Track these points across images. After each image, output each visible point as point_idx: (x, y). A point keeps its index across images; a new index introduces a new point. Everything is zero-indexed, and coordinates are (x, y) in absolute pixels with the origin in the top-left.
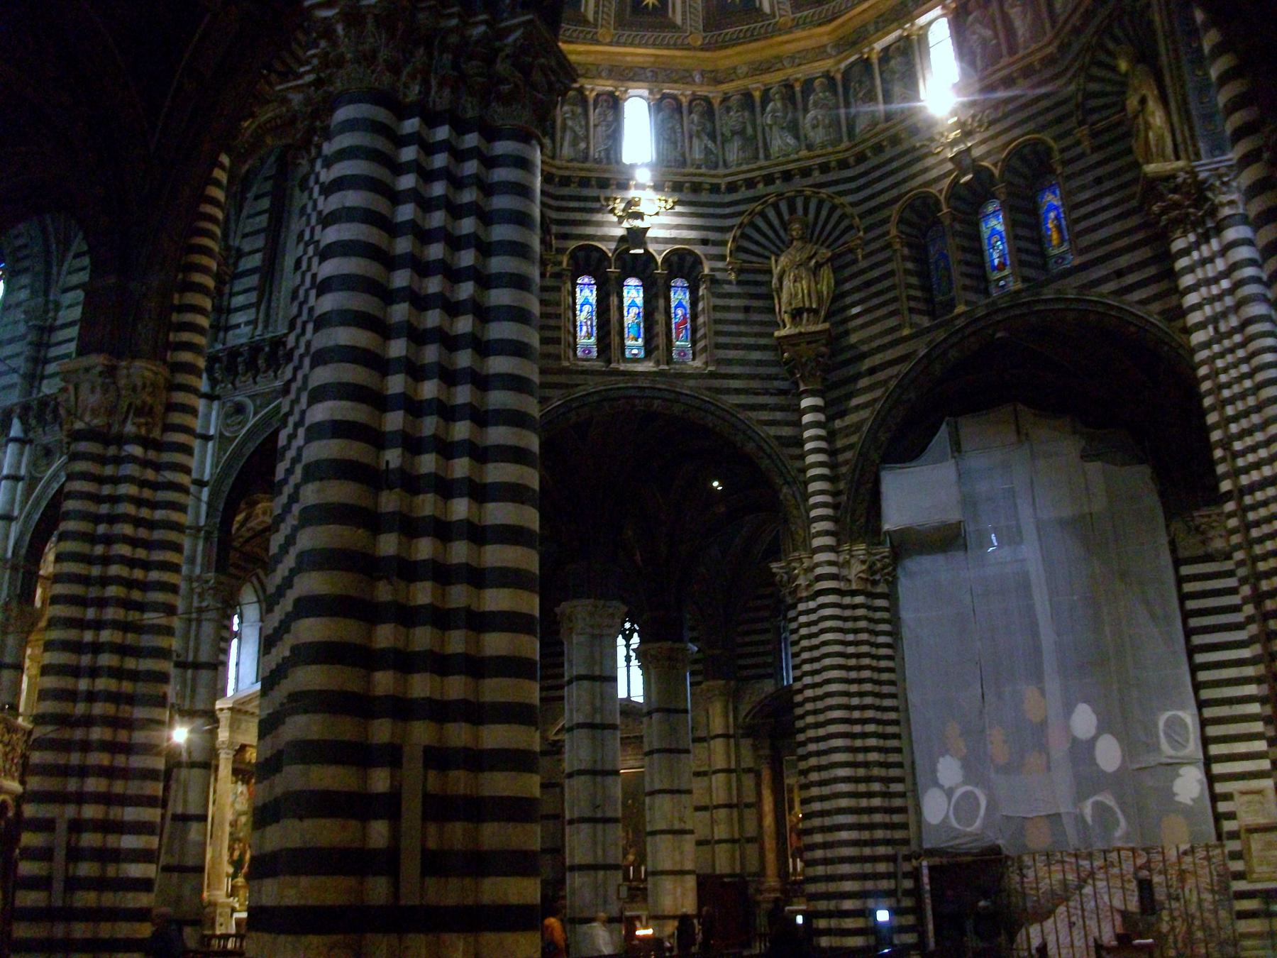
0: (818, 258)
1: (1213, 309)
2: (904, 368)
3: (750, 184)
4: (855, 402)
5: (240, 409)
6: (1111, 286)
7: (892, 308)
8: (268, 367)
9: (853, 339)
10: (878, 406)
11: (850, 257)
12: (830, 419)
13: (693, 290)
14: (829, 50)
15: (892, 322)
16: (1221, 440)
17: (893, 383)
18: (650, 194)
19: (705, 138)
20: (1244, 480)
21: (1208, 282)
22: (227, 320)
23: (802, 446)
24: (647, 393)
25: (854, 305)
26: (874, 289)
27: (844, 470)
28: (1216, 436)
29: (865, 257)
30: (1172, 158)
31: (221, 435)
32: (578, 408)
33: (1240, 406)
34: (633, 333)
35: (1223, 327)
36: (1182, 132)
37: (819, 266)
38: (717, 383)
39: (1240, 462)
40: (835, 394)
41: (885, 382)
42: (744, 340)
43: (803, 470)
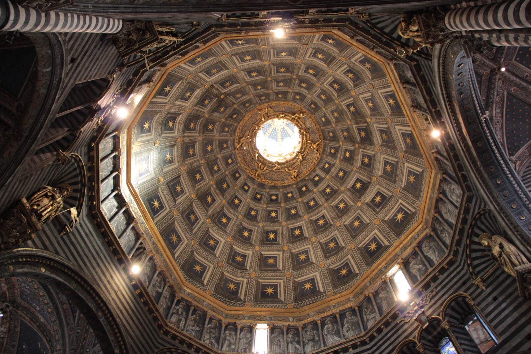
14: (351, 299)
19: (295, 344)
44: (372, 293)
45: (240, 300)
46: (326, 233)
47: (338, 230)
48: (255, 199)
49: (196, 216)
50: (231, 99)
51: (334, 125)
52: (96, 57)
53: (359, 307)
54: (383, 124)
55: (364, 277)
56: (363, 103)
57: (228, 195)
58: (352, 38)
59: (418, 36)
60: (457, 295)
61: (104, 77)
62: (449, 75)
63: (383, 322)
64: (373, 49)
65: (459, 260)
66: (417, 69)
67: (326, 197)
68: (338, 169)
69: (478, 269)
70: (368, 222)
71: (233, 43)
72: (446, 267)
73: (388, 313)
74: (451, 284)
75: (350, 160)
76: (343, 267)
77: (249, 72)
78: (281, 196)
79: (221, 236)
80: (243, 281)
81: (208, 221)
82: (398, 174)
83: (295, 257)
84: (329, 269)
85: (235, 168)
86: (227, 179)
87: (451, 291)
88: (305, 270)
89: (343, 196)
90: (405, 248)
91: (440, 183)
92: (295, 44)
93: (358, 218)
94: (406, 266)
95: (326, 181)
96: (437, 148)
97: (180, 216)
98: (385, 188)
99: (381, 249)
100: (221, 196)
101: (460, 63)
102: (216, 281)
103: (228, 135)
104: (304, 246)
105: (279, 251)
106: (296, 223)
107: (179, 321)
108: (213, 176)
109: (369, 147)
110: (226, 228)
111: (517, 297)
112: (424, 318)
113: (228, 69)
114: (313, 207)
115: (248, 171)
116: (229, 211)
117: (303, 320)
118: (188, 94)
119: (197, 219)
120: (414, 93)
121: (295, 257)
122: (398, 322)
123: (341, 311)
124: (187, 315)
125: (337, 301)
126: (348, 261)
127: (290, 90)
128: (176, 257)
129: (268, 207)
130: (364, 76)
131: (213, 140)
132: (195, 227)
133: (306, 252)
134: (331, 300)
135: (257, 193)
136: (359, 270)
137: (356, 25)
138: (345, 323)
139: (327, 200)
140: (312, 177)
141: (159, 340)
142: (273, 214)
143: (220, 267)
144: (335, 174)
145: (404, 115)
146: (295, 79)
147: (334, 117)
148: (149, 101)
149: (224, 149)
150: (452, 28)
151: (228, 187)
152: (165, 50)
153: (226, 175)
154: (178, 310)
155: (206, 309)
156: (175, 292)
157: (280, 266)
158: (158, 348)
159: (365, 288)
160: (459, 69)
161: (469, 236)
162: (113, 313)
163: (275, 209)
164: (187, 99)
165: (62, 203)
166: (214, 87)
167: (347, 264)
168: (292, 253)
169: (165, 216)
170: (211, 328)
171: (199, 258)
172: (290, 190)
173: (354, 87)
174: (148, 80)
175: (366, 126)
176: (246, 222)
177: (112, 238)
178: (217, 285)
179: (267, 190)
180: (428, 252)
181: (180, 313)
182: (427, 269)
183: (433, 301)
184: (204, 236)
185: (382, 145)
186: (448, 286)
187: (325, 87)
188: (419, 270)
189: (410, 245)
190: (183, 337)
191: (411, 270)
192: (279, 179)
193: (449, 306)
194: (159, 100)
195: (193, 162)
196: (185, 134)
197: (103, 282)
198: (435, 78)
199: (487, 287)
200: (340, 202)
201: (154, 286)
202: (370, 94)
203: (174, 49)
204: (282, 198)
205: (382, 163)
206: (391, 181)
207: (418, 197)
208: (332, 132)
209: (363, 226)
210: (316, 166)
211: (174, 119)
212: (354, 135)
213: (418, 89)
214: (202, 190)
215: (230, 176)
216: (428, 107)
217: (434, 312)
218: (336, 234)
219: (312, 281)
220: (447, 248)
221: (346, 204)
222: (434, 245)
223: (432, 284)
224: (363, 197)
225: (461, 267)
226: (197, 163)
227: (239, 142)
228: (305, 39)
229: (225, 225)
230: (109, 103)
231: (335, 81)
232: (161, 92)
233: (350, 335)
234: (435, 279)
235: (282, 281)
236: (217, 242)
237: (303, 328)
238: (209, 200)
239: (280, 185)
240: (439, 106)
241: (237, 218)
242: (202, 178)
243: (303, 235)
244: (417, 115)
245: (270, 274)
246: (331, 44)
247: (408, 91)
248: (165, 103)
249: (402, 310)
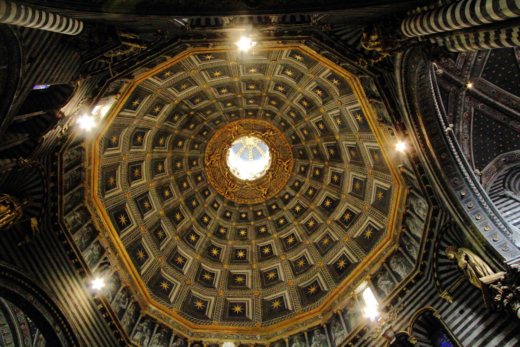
14: (319, 317)
44: (340, 310)
45: (207, 318)
47: (307, 248)
48: (224, 217)
49: (164, 233)
50: (201, 115)
51: (304, 143)
52: (57, 60)
54: (351, 141)
55: (333, 294)
56: (332, 120)
57: (198, 212)
58: (318, 52)
59: (378, 46)
60: (424, 310)
61: (67, 83)
62: (412, 86)
63: (351, 339)
64: (339, 64)
65: (426, 276)
66: (381, 83)
67: (295, 215)
69: (444, 283)
70: (338, 239)
71: (201, 57)
72: (413, 281)
73: (356, 330)
74: (418, 298)
75: (319, 178)
76: (312, 285)
77: (219, 88)
78: (250, 214)
79: (189, 254)
81: (177, 238)
83: (263, 276)
84: (298, 287)
85: (205, 185)
86: (197, 197)
87: (418, 306)
88: (274, 288)
89: (313, 214)
90: (373, 265)
91: (407, 198)
92: (264, 60)
93: (327, 236)
94: (374, 281)
95: (296, 199)
96: (404, 163)
97: (147, 232)
98: (355, 206)
99: (349, 266)
100: (190, 214)
101: (422, 73)
103: (197, 152)
104: (273, 264)
105: (248, 269)
106: (265, 241)
107: (143, 338)
108: (182, 193)
109: (338, 165)
110: (194, 246)
111: (484, 309)
113: (198, 85)
114: (282, 225)
115: (217, 189)
116: (198, 229)
117: (270, 338)
118: (157, 109)
120: (380, 108)
121: (263, 276)
122: (366, 339)
123: (309, 329)
124: (152, 333)
125: (305, 319)
127: (261, 108)
128: (142, 274)
129: (237, 225)
130: (332, 92)
131: (182, 157)
132: (163, 243)
133: (275, 270)
134: (300, 318)
135: (227, 211)
136: (328, 288)
137: (320, 38)
138: (313, 341)
139: (296, 218)
140: (282, 195)
142: (243, 233)
143: (188, 285)
144: (304, 192)
145: (371, 131)
146: (265, 96)
147: (304, 134)
148: (116, 114)
149: (194, 166)
150: (410, 35)
151: (198, 204)
152: (131, 60)
153: (196, 193)
154: (142, 328)
155: (171, 327)
156: (140, 309)
157: (249, 284)
160: (421, 80)
161: (436, 250)
162: (72, 327)
163: (244, 227)
164: (156, 114)
165: (21, 211)
166: (183, 103)
167: (316, 281)
168: (261, 272)
169: (132, 231)
172: (260, 209)
173: (323, 104)
174: (115, 92)
175: (335, 144)
177: (75, 251)
179: (237, 209)
180: (396, 268)
181: (144, 330)
182: (394, 284)
183: (400, 316)
185: (351, 162)
186: (416, 301)
187: (295, 105)
188: (387, 286)
191: (379, 286)
192: (249, 197)
193: (416, 321)
194: (127, 113)
195: (162, 178)
196: (154, 150)
197: (62, 296)
198: (397, 89)
199: (454, 301)
200: (310, 220)
201: (118, 302)
202: (338, 111)
203: (140, 59)
204: (252, 216)
205: (351, 180)
206: (360, 198)
207: (386, 213)
208: (302, 150)
209: (333, 244)
210: (286, 184)
211: (143, 135)
212: (323, 152)
213: (383, 103)
214: (171, 207)
216: (392, 119)
217: (401, 327)
218: (305, 252)
219: (281, 299)
220: (414, 263)
221: (315, 221)
222: (402, 261)
223: (400, 299)
225: (428, 282)
226: (167, 180)
227: (209, 159)
228: (273, 55)
229: (194, 243)
230: (73, 112)
231: (305, 98)
232: (129, 106)
234: (402, 294)
235: (250, 300)
236: (185, 260)
238: (178, 217)
239: (249, 203)
240: (403, 118)
241: (206, 236)
242: (171, 195)
243: (273, 253)
244: (382, 129)
245: (238, 292)
246: (299, 60)
247: (375, 105)
248: (134, 117)
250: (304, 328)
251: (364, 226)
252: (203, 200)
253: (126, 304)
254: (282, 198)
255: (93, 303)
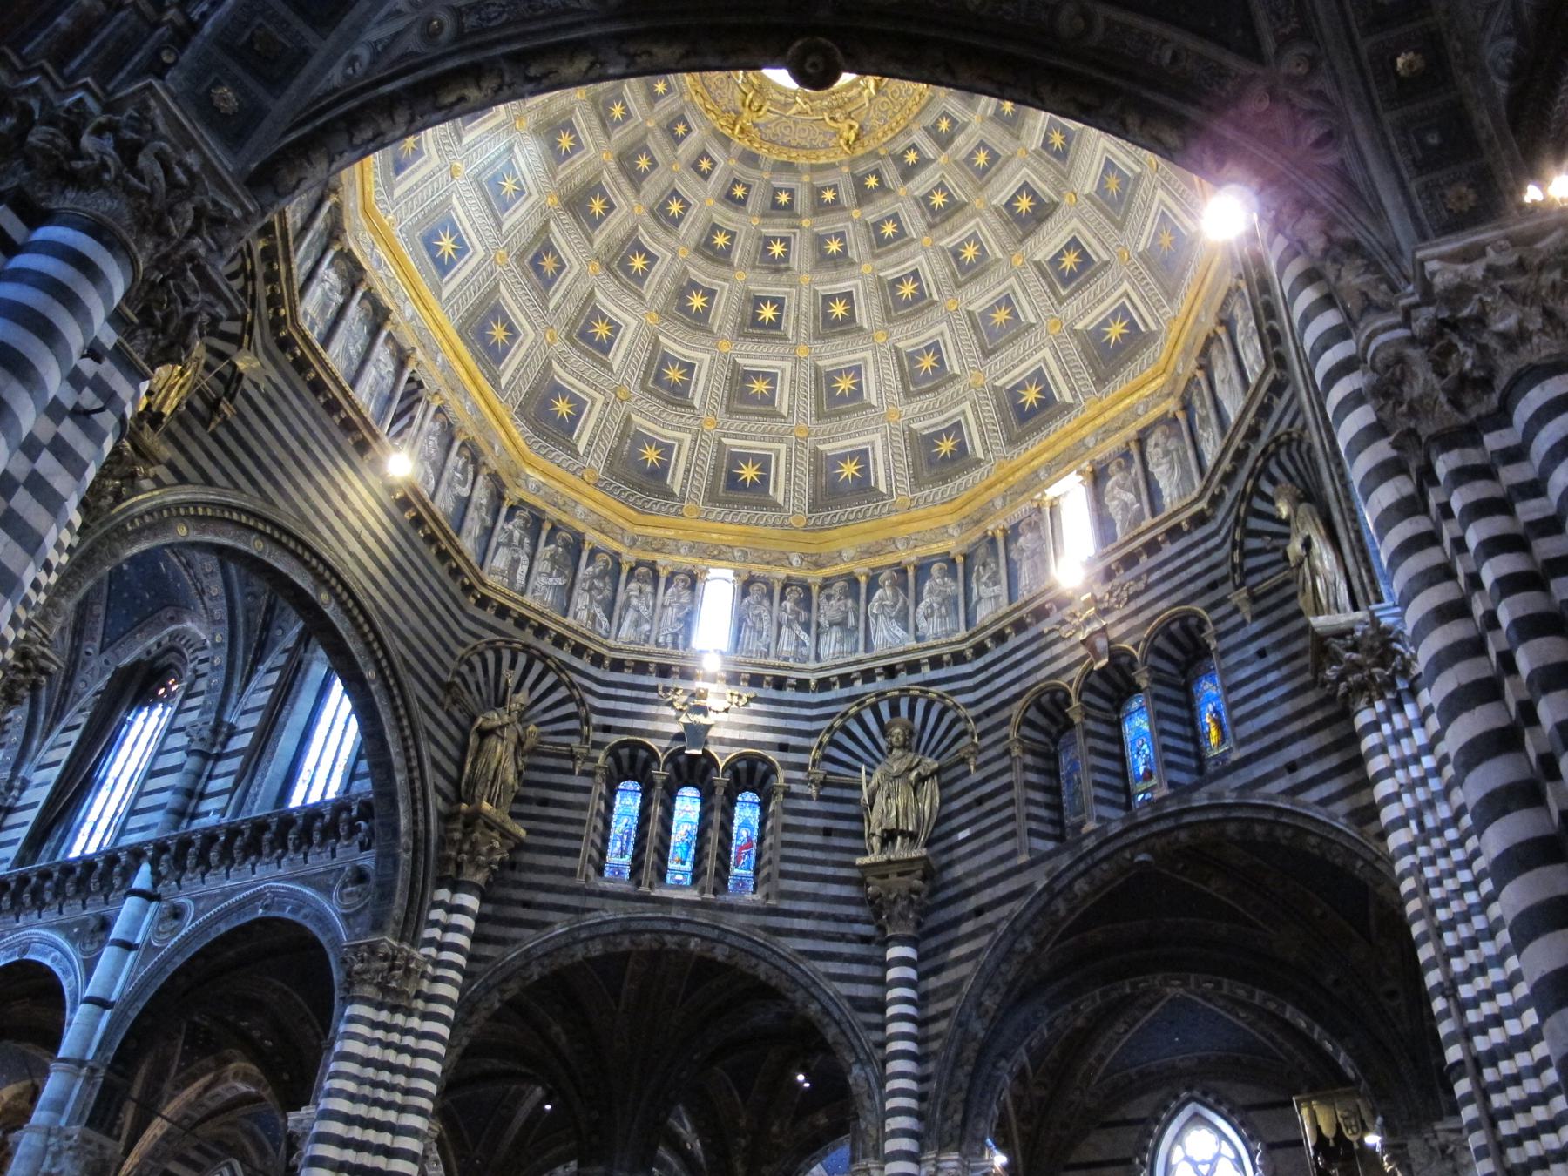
0: (920, 769)
1: (1415, 798)
2: (1018, 906)
3: (846, 680)
4: (955, 953)
5: (177, 913)
6: (1283, 783)
7: (1008, 828)
8: (221, 862)
9: (958, 871)
10: (983, 958)
11: (960, 770)
12: (923, 976)
13: (763, 806)
14: (950, 530)
15: (1007, 847)
16: (1440, 984)
17: (1004, 926)
18: (719, 687)
19: (797, 628)
20: (1481, 1044)
21: (1404, 763)
22: (196, 806)
23: (883, 1012)
24: (683, 927)
25: (962, 828)
26: (988, 806)
27: (935, 1046)
28: (1433, 978)
29: (977, 768)
30: (1349, 608)
31: (150, 944)
32: (586, 940)
33: (1464, 931)
34: (680, 854)
35: (1430, 822)
36: (1360, 577)
37: (922, 779)
38: (774, 921)
39: (1472, 1016)
40: (933, 942)
41: (991, 927)
42: (819, 870)
43: (882, 1045)
46: (917, 323)
47: (949, 322)
48: (729, 198)
53: (965, 557)
57: (652, 189)
65: (1219, 519)
67: (929, 217)
68: (974, 141)
70: (1033, 320)
73: (1026, 603)
74: (1184, 575)
76: (947, 431)
80: (681, 441)
81: (595, 268)
82: (1134, 208)
83: (824, 381)
84: (910, 429)
85: (674, 107)
87: (1179, 596)
88: (847, 421)
93: (1007, 301)
97: (514, 265)
98: (1095, 235)
102: (611, 440)
104: (852, 352)
105: (783, 358)
106: (838, 281)
107: (514, 564)
112: (1101, 643)
116: (652, 237)
119: (561, 267)
121: (824, 381)
124: (535, 546)
125: (915, 527)
126: (961, 418)
129: (764, 226)
134: (902, 523)
135: (736, 182)
136: (986, 451)
139: (931, 226)
140: (899, 150)
141: (467, 623)
142: (777, 249)
144: (963, 154)
151: (654, 164)
153: (648, 131)
155: (580, 527)
156: (503, 486)
157: (783, 404)
158: (463, 644)
159: (985, 513)
161: (1256, 474)
163: (783, 232)
167: (958, 425)
170: (594, 577)
171: (562, 375)
172: (831, 181)
176: (699, 268)
178: (614, 453)
179: (766, 176)
183: (1133, 605)
184: (581, 311)
188: (1125, 507)
189: (1120, 428)
190: (524, 611)
193: (1164, 630)
200: (968, 240)
204: (807, 201)
206: (1113, 222)
209: (1017, 329)
214: (577, 180)
215: (658, 133)
218: (942, 334)
223: (1144, 558)
224: (1030, 242)
229: (640, 278)
233: (932, 628)
234: (1152, 547)
235: (783, 447)
236: (615, 328)
237: (822, 588)
239: (803, 161)
242: (577, 146)
243: (854, 321)
245: (753, 424)
249: (1062, 603)
250: (909, 556)
251: (1108, 305)
252: (668, 151)
253: (469, 485)
254: (899, 158)
255: (395, 511)
